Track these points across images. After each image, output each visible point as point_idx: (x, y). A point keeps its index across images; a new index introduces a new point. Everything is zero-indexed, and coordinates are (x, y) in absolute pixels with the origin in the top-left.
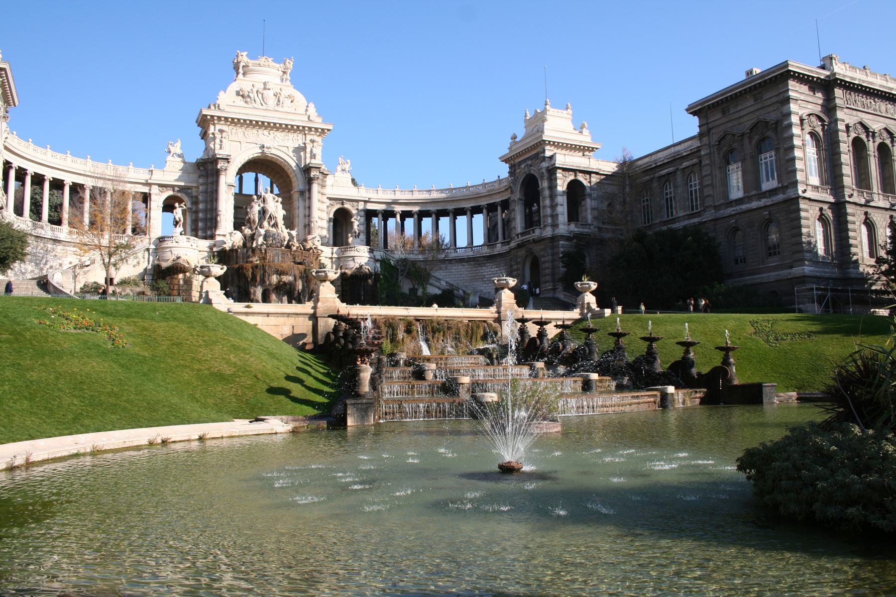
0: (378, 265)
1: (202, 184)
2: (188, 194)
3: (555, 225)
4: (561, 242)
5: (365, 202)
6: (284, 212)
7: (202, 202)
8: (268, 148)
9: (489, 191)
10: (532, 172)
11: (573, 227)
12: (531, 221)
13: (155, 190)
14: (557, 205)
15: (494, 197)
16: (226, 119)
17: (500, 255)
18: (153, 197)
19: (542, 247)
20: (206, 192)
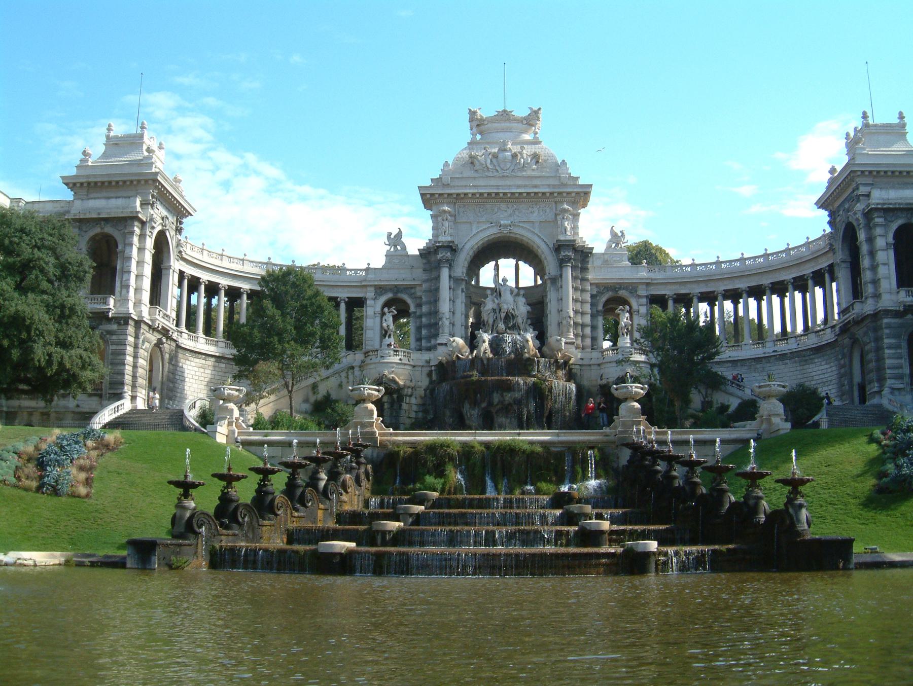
0: (656, 371)
1: (425, 281)
2: (411, 295)
3: (877, 296)
4: (885, 321)
5: (648, 284)
6: (529, 308)
7: (426, 303)
8: (506, 226)
9: (813, 253)
10: (850, 220)
12: (857, 292)
13: (370, 294)
14: (878, 265)
15: (820, 260)
17: (829, 345)
18: (369, 302)
19: (865, 329)
20: (430, 291)
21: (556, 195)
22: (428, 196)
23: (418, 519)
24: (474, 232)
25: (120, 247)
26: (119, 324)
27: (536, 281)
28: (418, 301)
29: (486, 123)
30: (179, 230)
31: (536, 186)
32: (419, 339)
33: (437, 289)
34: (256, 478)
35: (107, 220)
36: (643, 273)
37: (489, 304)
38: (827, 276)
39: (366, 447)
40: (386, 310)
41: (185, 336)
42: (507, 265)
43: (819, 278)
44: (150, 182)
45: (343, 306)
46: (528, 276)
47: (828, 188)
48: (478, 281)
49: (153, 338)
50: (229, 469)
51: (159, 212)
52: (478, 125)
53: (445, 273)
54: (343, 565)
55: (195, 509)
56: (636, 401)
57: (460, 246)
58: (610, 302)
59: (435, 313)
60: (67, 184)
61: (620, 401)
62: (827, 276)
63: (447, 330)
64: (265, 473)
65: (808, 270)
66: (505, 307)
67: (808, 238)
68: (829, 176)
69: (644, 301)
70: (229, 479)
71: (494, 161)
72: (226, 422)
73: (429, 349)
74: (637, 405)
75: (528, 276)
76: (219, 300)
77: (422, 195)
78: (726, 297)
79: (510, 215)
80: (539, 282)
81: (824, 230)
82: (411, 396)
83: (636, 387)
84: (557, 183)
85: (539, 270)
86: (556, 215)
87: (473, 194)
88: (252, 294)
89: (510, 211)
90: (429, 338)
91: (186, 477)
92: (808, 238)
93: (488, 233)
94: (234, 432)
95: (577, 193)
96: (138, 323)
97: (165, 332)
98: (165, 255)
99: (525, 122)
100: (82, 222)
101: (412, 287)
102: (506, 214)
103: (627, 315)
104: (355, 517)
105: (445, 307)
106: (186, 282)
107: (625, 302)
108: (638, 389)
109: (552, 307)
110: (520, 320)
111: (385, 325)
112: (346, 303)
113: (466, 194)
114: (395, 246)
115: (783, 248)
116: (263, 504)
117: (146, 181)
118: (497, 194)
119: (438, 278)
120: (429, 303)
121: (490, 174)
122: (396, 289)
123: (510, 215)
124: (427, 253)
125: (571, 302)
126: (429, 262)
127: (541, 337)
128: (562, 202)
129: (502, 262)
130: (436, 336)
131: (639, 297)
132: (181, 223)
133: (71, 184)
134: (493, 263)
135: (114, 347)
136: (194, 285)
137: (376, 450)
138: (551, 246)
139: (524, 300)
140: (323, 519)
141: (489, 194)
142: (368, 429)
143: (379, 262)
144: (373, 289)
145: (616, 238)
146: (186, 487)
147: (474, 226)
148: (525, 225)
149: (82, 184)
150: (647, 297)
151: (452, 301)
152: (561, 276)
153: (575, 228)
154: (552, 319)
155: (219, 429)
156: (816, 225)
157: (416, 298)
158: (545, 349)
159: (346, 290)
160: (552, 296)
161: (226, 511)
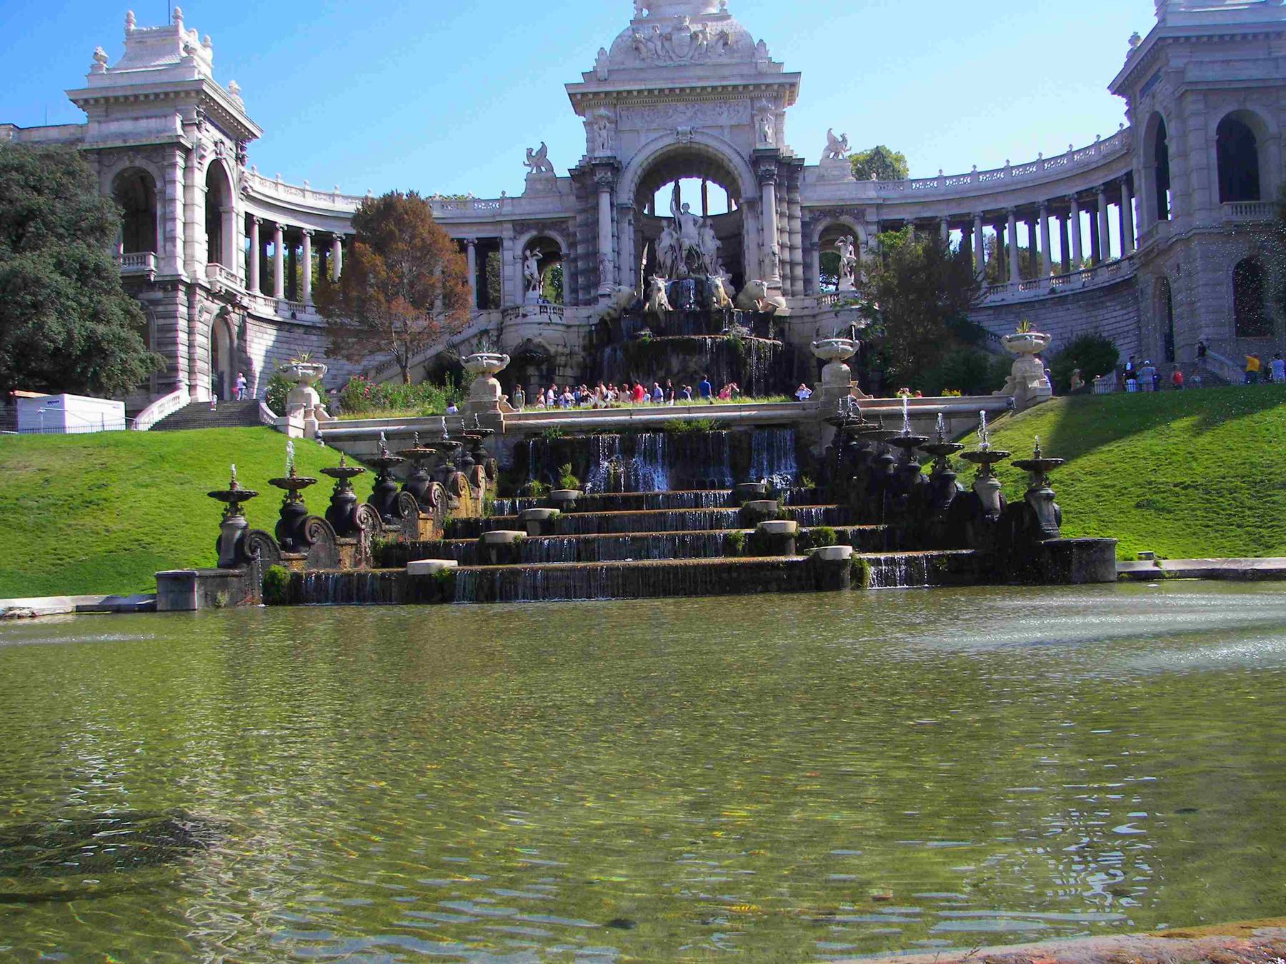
5: (879, 206)
6: (719, 243)
8: (684, 134)
11: (1226, 212)
13: (507, 233)
18: (506, 244)
20: (586, 225)
22: (579, 97)
23: (548, 526)
24: (643, 142)
25: (159, 184)
26: (165, 290)
27: (729, 206)
28: (571, 240)
30: (240, 159)
31: (724, 78)
32: (574, 291)
33: (596, 222)
34: (330, 483)
35: (136, 149)
36: (870, 192)
37: (666, 240)
38: (1124, 189)
39: (485, 435)
40: (528, 253)
41: (260, 301)
42: (690, 187)
43: (1113, 192)
44: (193, 94)
45: (471, 250)
46: (719, 202)
47: (1126, 64)
48: (652, 209)
49: (216, 307)
50: (292, 471)
51: (209, 135)
53: (605, 200)
54: (437, 591)
55: (246, 527)
56: (844, 362)
57: (624, 164)
58: (826, 232)
59: (594, 255)
60: (75, 101)
61: (822, 363)
62: (1124, 189)
63: (610, 277)
64: (342, 476)
65: (1098, 180)
66: (687, 243)
67: (1098, 136)
68: (1129, 47)
69: (874, 228)
70: (292, 486)
71: (667, 44)
72: (302, 411)
73: (588, 303)
74: (845, 367)
75: (719, 202)
76: (276, 247)
78: (985, 222)
79: (690, 119)
80: (734, 208)
81: (1121, 125)
82: (565, 366)
83: (843, 343)
84: (753, 71)
85: (733, 193)
86: (752, 116)
87: (639, 92)
88: (348, 242)
89: (689, 113)
90: (587, 288)
91: (233, 485)
92: (1098, 136)
93: (661, 144)
94: (313, 425)
95: (781, 85)
96: (191, 288)
97: (229, 298)
98: (224, 194)
100: (102, 155)
101: (563, 221)
103: (851, 248)
104: (471, 527)
105: (606, 245)
106: (256, 228)
107: (848, 231)
108: (846, 346)
109: (750, 241)
110: (707, 260)
111: (527, 273)
112: (475, 245)
113: (629, 92)
114: (538, 167)
115: (1065, 150)
116: (340, 518)
117: (187, 93)
118: (671, 90)
119: (596, 208)
120: (585, 241)
121: (662, 63)
122: (541, 224)
123: (690, 119)
124: (581, 174)
125: (776, 232)
126: (583, 186)
127: (737, 281)
128: (760, 98)
129: (683, 182)
130: (596, 285)
131: (868, 223)
132: (243, 149)
133: (84, 103)
134: (671, 185)
135: (161, 322)
136: (268, 231)
137: (501, 439)
138: (747, 159)
139: (712, 233)
140: (428, 531)
141: (661, 90)
142: (492, 412)
143: (517, 188)
144: (510, 226)
145: (836, 145)
146: (233, 499)
149: (96, 100)
150: (878, 223)
151: (616, 237)
152: (761, 197)
153: (778, 132)
154: (751, 257)
155: (292, 421)
156: (1109, 117)
157: (568, 235)
158: (741, 297)
159: (475, 228)
160: (750, 225)
161: (292, 525)
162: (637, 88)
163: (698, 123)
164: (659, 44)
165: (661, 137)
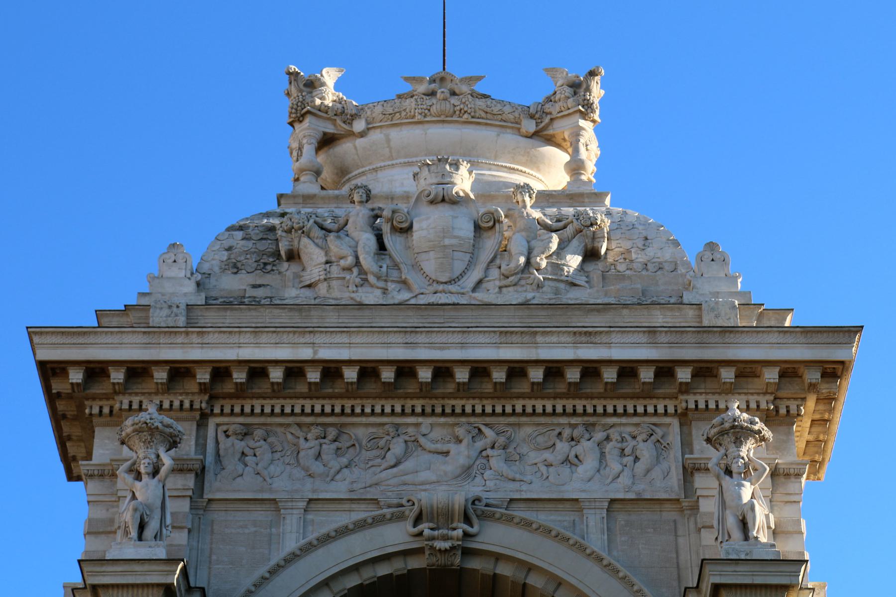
16: (180, 371)
21: (684, 375)
22: (76, 376)
24: (291, 544)
29: (359, 126)
52: (326, 142)
77: (49, 371)
86: (689, 471)
87: (294, 370)
89: (461, 454)
95: (790, 372)
99: (530, 126)
102: (450, 466)
113: (257, 370)
118: (406, 370)
121: (370, 296)
123: (466, 472)
141: (369, 370)
147: (292, 522)
148: (543, 517)
162: (284, 353)
163: (489, 486)
164: (367, 240)
165: (361, 526)
